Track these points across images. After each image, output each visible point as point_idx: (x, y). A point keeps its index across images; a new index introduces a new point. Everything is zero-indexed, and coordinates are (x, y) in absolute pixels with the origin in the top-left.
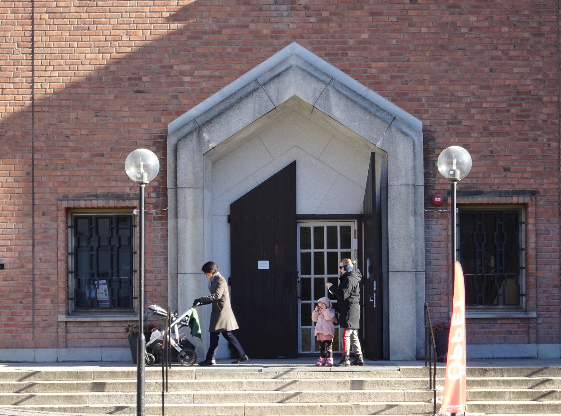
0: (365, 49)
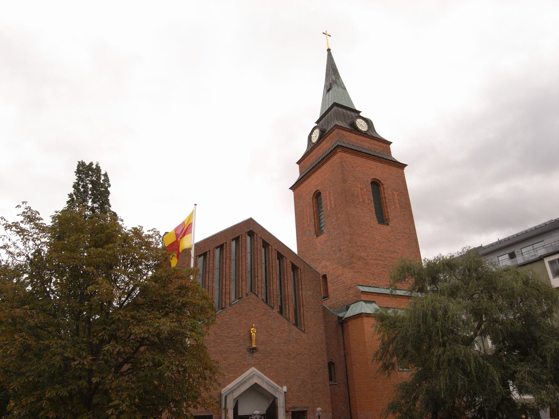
0: (269, 369)
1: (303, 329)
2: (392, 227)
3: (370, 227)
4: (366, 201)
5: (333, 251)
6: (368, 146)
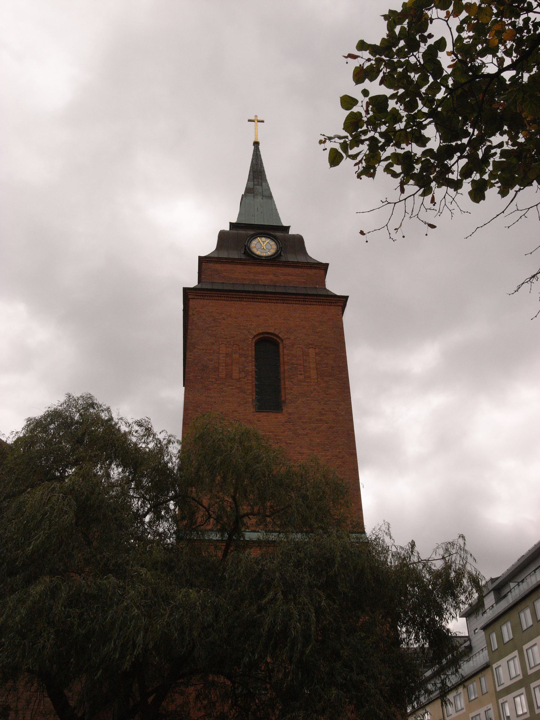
4: (236, 375)
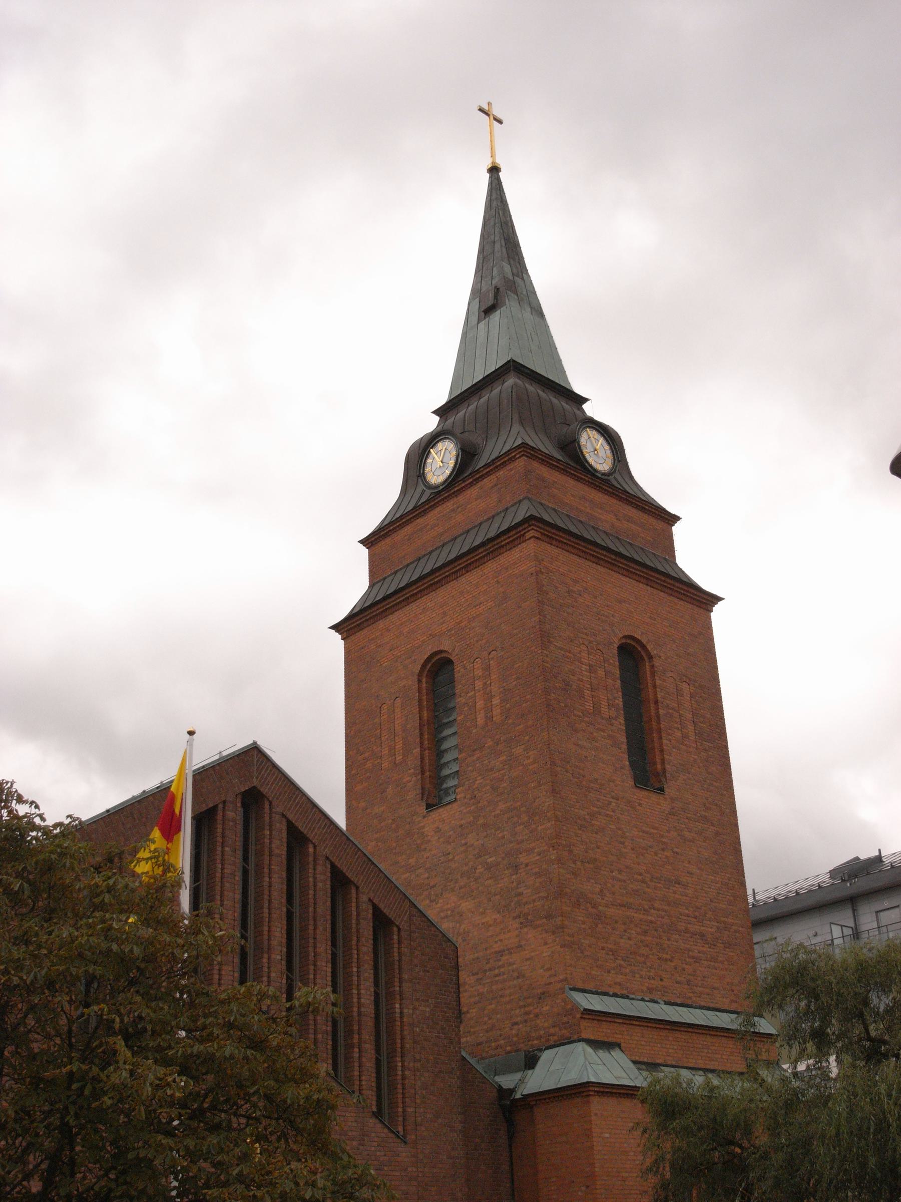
1: (400, 1129)
2: (673, 800)
3: (613, 798)
4: (604, 709)
5: (489, 867)
6: (613, 526)
